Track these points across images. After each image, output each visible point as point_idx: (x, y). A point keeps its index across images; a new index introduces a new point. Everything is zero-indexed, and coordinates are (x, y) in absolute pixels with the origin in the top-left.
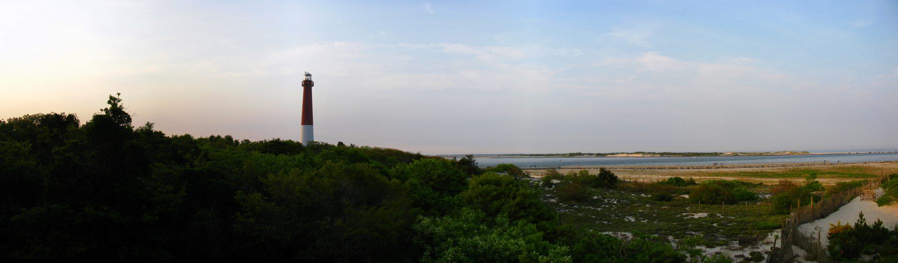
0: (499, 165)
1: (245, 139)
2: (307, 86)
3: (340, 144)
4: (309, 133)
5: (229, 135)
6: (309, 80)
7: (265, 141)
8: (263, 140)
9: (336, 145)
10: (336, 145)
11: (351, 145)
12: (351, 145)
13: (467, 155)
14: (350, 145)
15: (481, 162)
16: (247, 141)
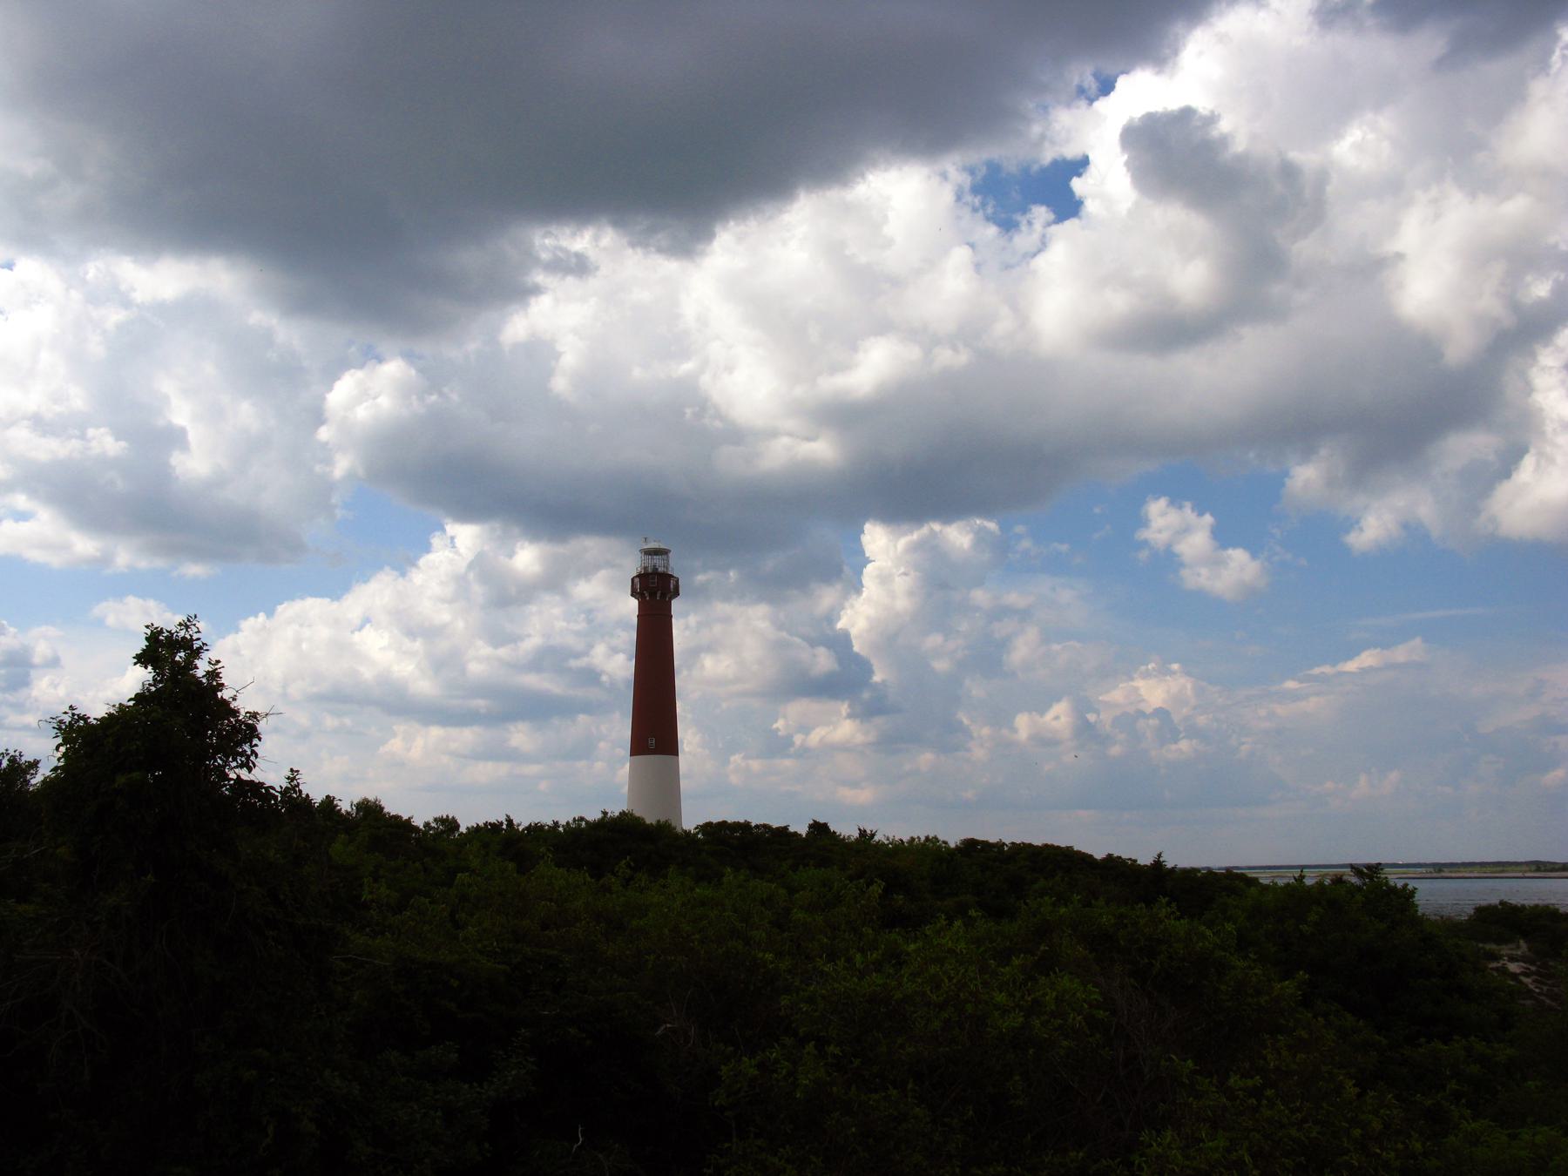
0: (1480, 910)
1: (438, 815)
2: (653, 595)
3: (819, 829)
4: (669, 786)
5: (371, 798)
6: (661, 570)
7: (510, 822)
8: (503, 819)
9: (802, 829)
10: (802, 829)
11: (863, 833)
12: (863, 833)
13: (1352, 866)
14: (856, 834)
15: (1432, 898)
16: (450, 824)
